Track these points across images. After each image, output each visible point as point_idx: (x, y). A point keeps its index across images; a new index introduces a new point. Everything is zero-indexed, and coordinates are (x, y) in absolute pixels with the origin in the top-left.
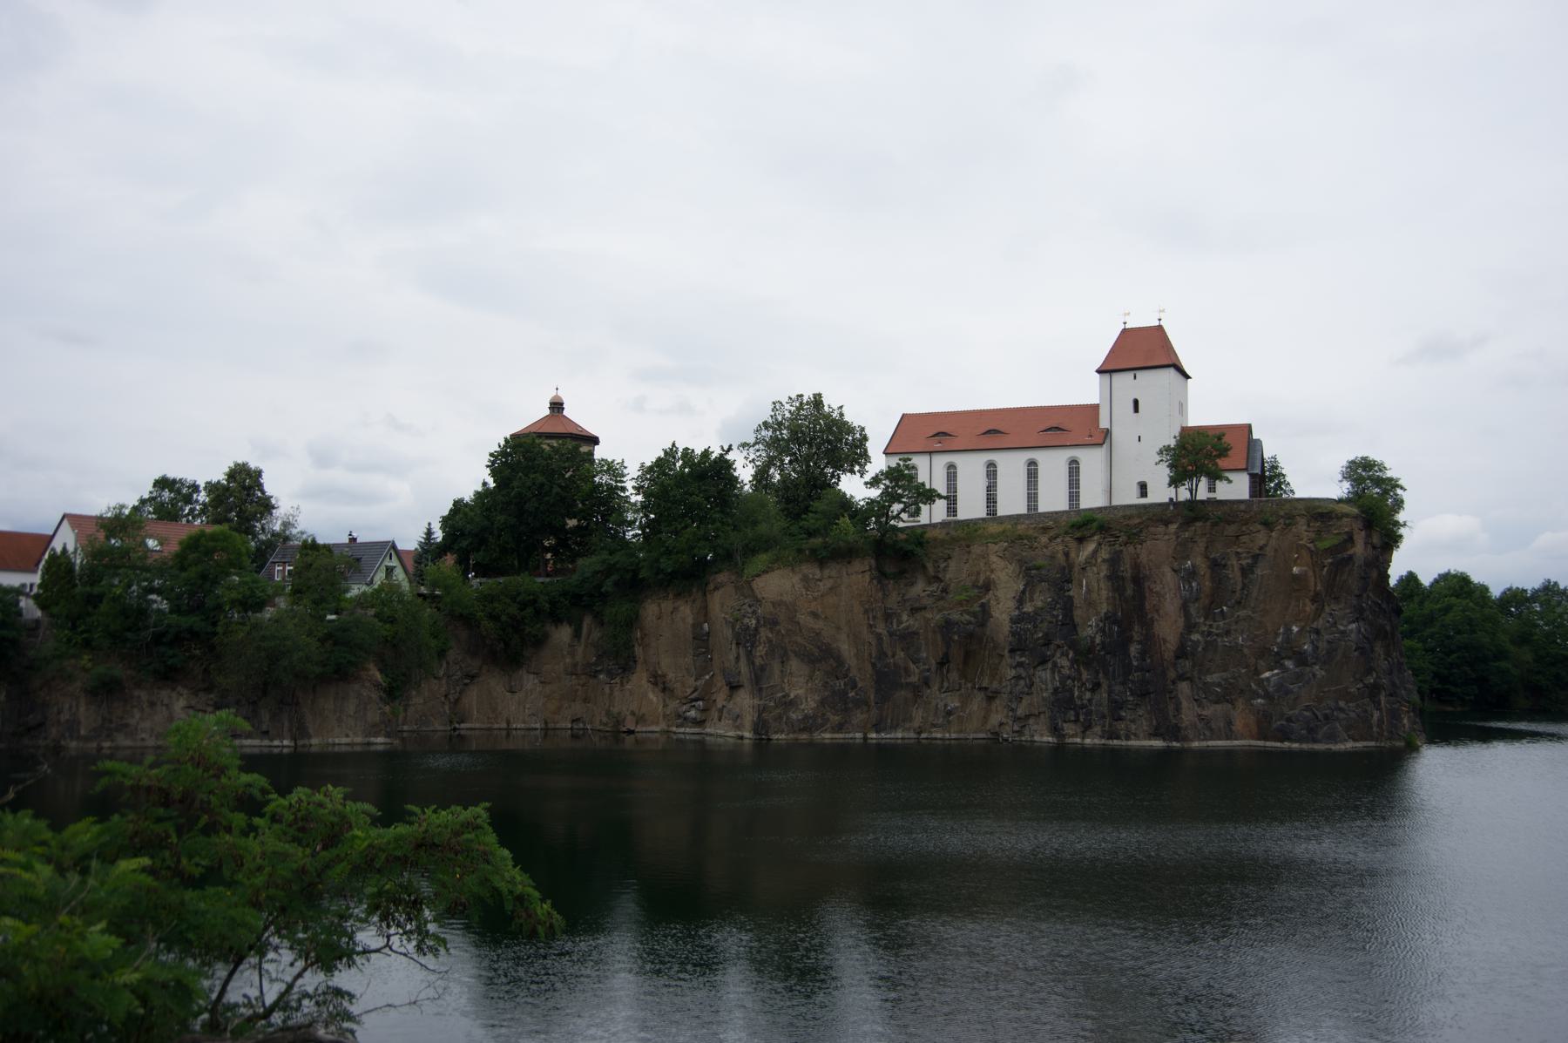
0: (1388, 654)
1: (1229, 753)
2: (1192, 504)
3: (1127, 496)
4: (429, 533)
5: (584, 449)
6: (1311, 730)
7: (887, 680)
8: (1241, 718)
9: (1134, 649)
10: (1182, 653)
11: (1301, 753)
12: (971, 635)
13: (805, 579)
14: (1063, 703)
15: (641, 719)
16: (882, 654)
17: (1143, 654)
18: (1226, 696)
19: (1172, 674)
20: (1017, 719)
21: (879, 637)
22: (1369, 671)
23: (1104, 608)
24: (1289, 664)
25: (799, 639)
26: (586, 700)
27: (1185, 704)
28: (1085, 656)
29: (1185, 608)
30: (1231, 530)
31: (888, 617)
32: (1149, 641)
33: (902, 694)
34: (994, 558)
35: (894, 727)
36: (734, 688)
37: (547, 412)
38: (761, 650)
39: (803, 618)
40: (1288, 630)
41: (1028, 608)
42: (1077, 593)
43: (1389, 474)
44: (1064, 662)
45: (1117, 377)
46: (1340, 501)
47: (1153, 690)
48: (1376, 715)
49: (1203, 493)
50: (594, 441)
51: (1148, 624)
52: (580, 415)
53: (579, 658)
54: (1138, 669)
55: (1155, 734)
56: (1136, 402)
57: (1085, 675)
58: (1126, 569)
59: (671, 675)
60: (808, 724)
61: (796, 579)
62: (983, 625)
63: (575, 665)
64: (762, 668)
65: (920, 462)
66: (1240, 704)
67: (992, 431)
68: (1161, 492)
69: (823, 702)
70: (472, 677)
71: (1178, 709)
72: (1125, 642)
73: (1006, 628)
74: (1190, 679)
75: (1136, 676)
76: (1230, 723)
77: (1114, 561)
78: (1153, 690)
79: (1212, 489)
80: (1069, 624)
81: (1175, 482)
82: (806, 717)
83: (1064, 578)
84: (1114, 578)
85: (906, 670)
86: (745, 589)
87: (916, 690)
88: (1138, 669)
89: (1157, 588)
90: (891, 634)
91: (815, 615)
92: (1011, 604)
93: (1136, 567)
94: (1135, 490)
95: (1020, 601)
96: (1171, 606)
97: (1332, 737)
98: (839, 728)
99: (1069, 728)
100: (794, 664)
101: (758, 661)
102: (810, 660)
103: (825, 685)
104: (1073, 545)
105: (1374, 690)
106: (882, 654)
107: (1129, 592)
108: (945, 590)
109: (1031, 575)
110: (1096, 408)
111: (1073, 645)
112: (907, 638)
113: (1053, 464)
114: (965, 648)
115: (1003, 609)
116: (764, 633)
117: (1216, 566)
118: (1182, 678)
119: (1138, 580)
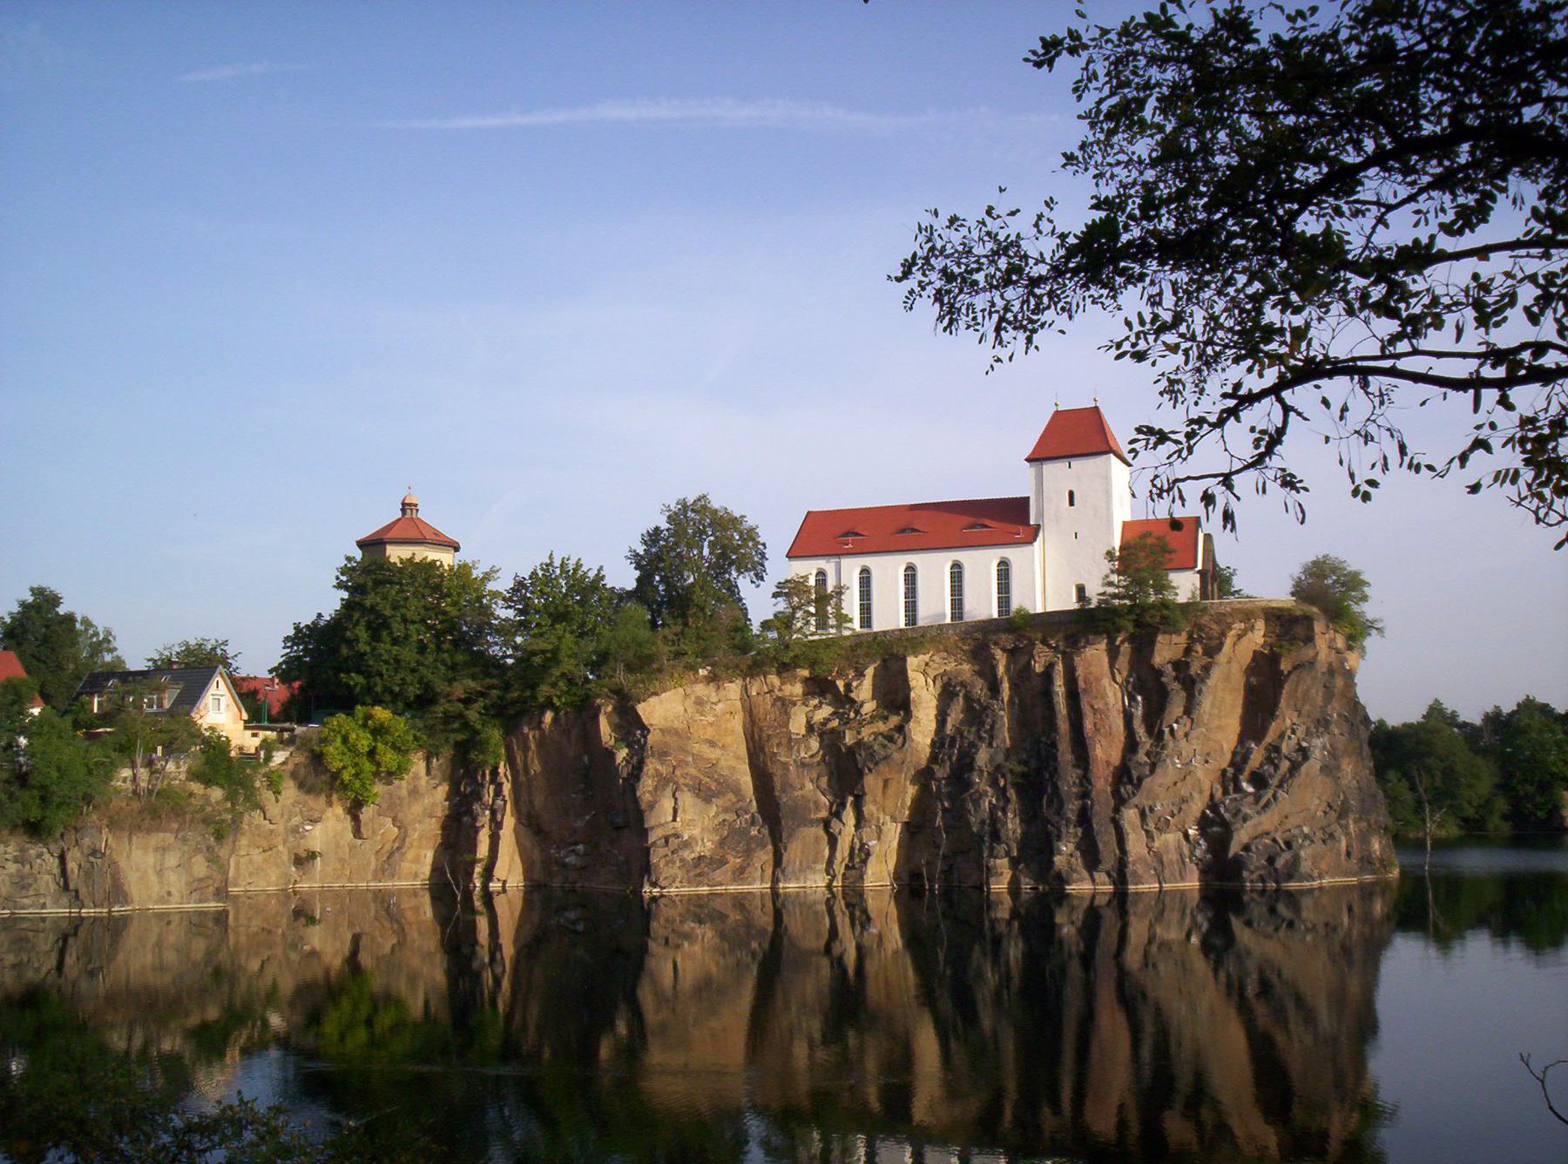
13: (700, 702)
25: (693, 771)
34: (911, 674)
37: (399, 515)
45: (1048, 468)
56: (1071, 494)
69: (722, 843)
85: (816, 803)
89: (1099, 705)
91: (712, 744)
92: (933, 726)
100: (687, 799)
113: (981, 565)
116: (651, 765)
119: (1073, 695)
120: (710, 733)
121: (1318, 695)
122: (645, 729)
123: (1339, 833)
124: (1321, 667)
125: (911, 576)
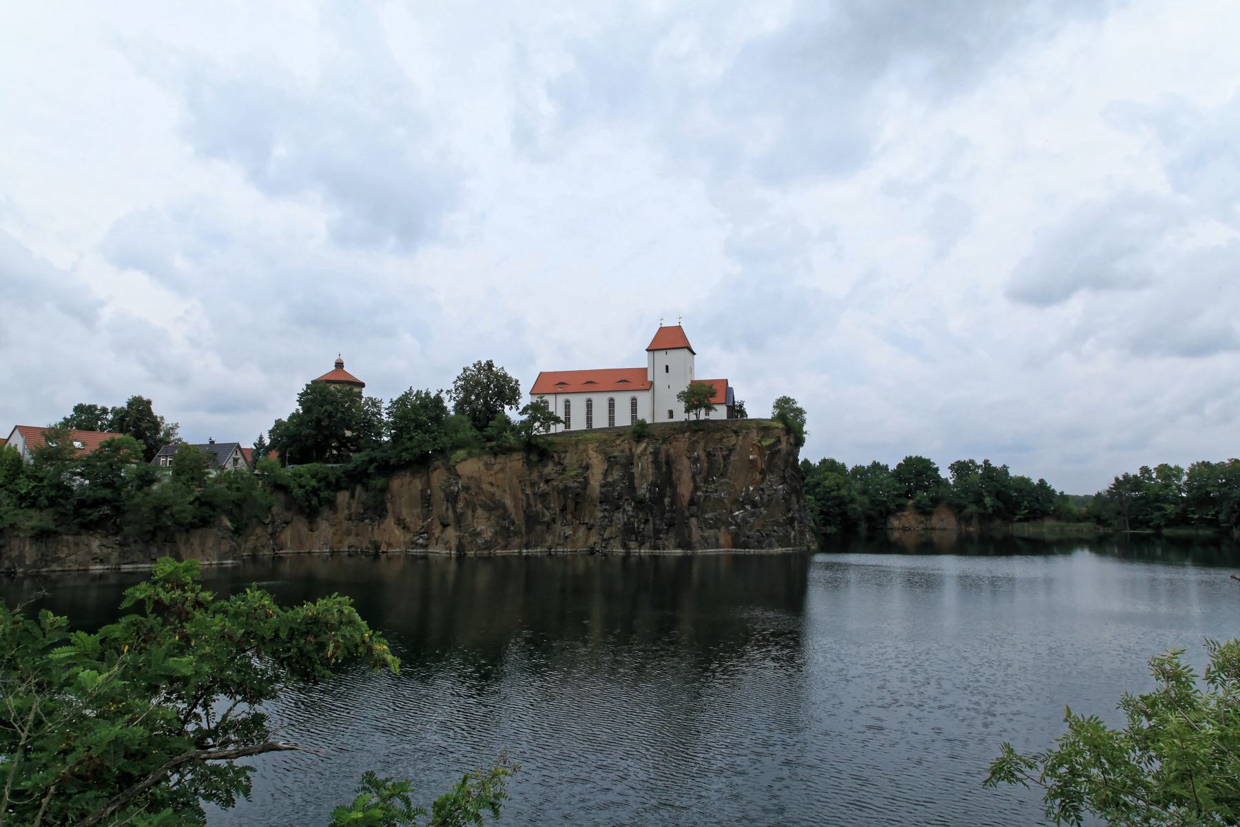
0: (798, 501)
1: (717, 557)
2: (697, 422)
3: (663, 418)
4: (261, 438)
5: (356, 390)
6: (759, 542)
7: (532, 519)
8: (724, 537)
9: (667, 500)
10: (692, 502)
11: (754, 556)
12: (577, 495)
13: (486, 464)
14: (629, 531)
15: (389, 545)
16: (529, 505)
17: (672, 503)
18: (716, 525)
19: (687, 514)
20: (603, 540)
21: (527, 495)
22: (789, 510)
23: (651, 478)
24: (748, 507)
25: (482, 498)
26: (357, 535)
27: (694, 530)
28: (640, 504)
29: (693, 478)
30: (718, 436)
31: (533, 485)
32: (675, 497)
33: (538, 527)
34: (591, 452)
35: (536, 546)
36: (445, 526)
38: (461, 504)
39: (486, 487)
40: (748, 489)
41: (610, 479)
42: (636, 471)
43: (799, 405)
44: (629, 508)
45: (657, 353)
46: (772, 420)
47: (675, 525)
48: (793, 533)
49: (702, 416)
50: (363, 385)
51: (674, 487)
52: (354, 370)
53: (353, 510)
54: (670, 511)
55: (679, 546)
57: (641, 516)
58: (662, 458)
59: (408, 520)
60: (489, 545)
61: (481, 464)
62: (585, 489)
63: (350, 515)
64: (462, 514)
65: (550, 399)
66: (723, 529)
67: (590, 382)
68: (681, 416)
69: (496, 533)
70: (287, 523)
71: (690, 533)
72: (662, 496)
73: (598, 490)
74: (697, 516)
75: (667, 515)
76: (717, 540)
77: (656, 454)
78: (675, 525)
79: (707, 414)
80: (632, 488)
81: (687, 411)
82: (487, 542)
83: (630, 462)
84: (656, 462)
85: (543, 515)
86: (452, 470)
87: (548, 526)
88: (670, 511)
89: (679, 467)
90: (534, 494)
91: (492, 484)
92: (600, 477)
93: (668, 456)
94: (667, 414)
95: (605, 475)
96: (686, 477)
97: (770, 546)
98: (505, 547)
99: (632, 544)
100: (480, 512)
101: (459, 511)
102: (489, 509)
103: (498, 523)
104: (634, 444)
105: (792, 520)
106: (529, 505)
107: (664, 469)
108: (564, 470)
109: (611, 461)
110: (644, 371)
111: (634, 499)
112: (543, 496)
113: (623, 401)
114: (574, 501)
115: (596, 481)
116: (463, 495)
117: (709, 455)
118: (692, 516)
119: (668, 463)
120: (491, 479)
121: (781, 465)
122: (459, 477)
123: (790, 529)
124: (783, 452)
125: (589, 405)
